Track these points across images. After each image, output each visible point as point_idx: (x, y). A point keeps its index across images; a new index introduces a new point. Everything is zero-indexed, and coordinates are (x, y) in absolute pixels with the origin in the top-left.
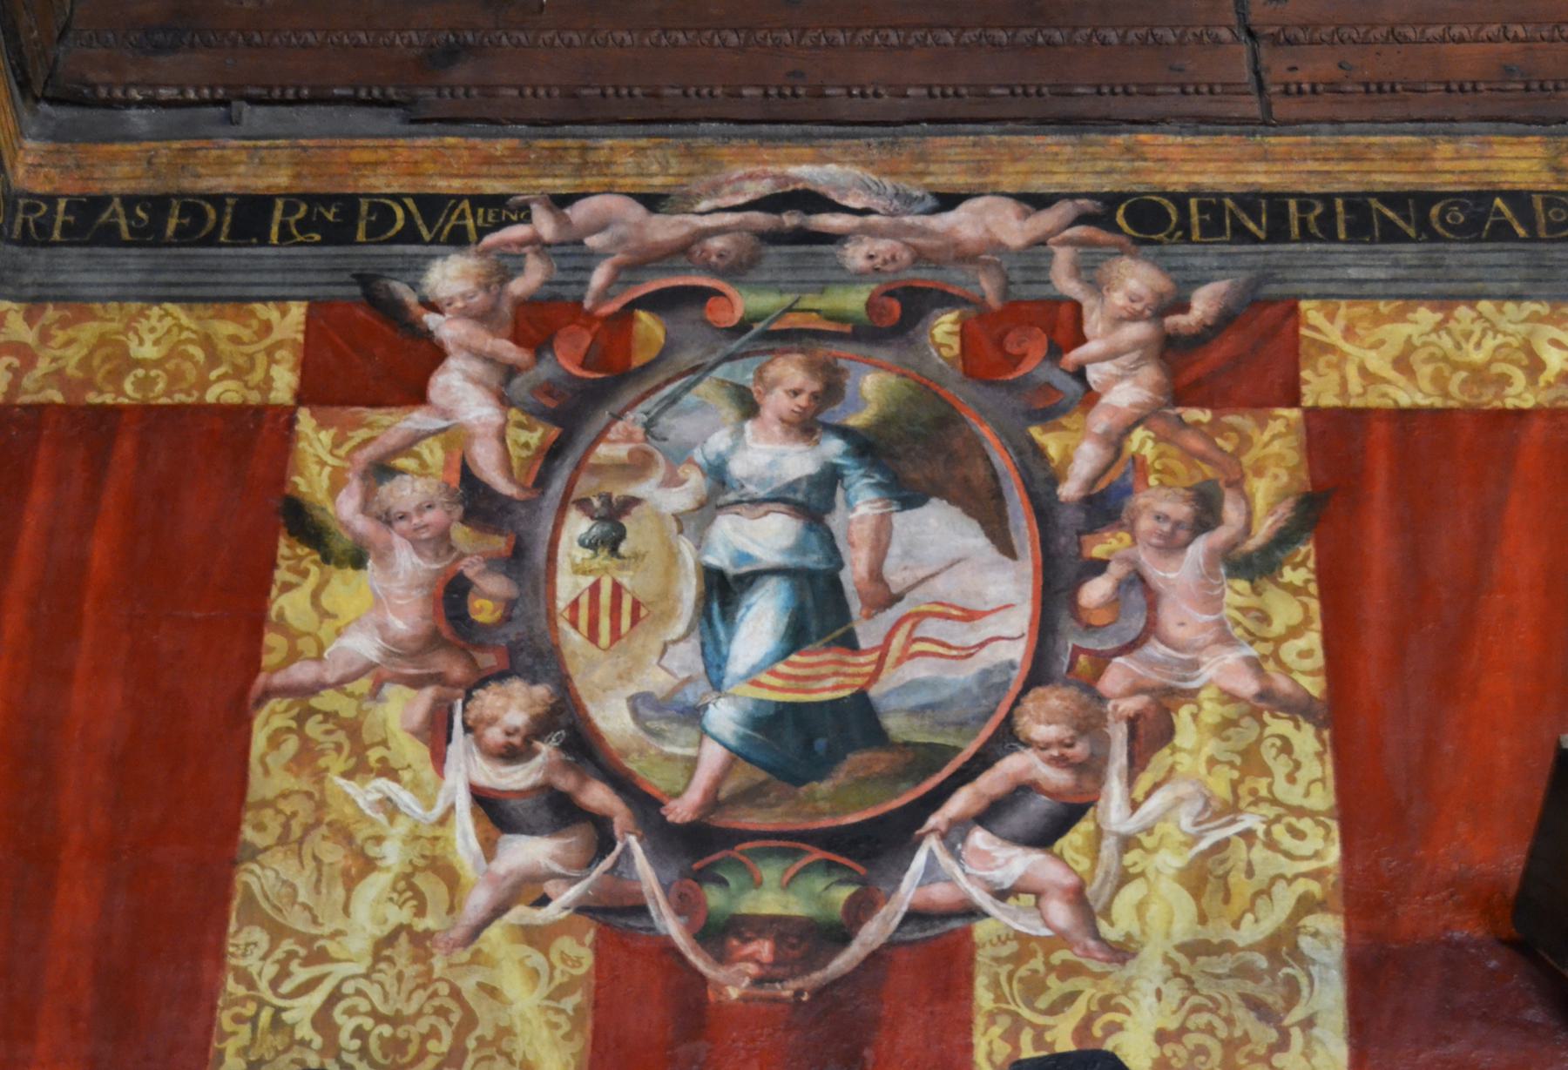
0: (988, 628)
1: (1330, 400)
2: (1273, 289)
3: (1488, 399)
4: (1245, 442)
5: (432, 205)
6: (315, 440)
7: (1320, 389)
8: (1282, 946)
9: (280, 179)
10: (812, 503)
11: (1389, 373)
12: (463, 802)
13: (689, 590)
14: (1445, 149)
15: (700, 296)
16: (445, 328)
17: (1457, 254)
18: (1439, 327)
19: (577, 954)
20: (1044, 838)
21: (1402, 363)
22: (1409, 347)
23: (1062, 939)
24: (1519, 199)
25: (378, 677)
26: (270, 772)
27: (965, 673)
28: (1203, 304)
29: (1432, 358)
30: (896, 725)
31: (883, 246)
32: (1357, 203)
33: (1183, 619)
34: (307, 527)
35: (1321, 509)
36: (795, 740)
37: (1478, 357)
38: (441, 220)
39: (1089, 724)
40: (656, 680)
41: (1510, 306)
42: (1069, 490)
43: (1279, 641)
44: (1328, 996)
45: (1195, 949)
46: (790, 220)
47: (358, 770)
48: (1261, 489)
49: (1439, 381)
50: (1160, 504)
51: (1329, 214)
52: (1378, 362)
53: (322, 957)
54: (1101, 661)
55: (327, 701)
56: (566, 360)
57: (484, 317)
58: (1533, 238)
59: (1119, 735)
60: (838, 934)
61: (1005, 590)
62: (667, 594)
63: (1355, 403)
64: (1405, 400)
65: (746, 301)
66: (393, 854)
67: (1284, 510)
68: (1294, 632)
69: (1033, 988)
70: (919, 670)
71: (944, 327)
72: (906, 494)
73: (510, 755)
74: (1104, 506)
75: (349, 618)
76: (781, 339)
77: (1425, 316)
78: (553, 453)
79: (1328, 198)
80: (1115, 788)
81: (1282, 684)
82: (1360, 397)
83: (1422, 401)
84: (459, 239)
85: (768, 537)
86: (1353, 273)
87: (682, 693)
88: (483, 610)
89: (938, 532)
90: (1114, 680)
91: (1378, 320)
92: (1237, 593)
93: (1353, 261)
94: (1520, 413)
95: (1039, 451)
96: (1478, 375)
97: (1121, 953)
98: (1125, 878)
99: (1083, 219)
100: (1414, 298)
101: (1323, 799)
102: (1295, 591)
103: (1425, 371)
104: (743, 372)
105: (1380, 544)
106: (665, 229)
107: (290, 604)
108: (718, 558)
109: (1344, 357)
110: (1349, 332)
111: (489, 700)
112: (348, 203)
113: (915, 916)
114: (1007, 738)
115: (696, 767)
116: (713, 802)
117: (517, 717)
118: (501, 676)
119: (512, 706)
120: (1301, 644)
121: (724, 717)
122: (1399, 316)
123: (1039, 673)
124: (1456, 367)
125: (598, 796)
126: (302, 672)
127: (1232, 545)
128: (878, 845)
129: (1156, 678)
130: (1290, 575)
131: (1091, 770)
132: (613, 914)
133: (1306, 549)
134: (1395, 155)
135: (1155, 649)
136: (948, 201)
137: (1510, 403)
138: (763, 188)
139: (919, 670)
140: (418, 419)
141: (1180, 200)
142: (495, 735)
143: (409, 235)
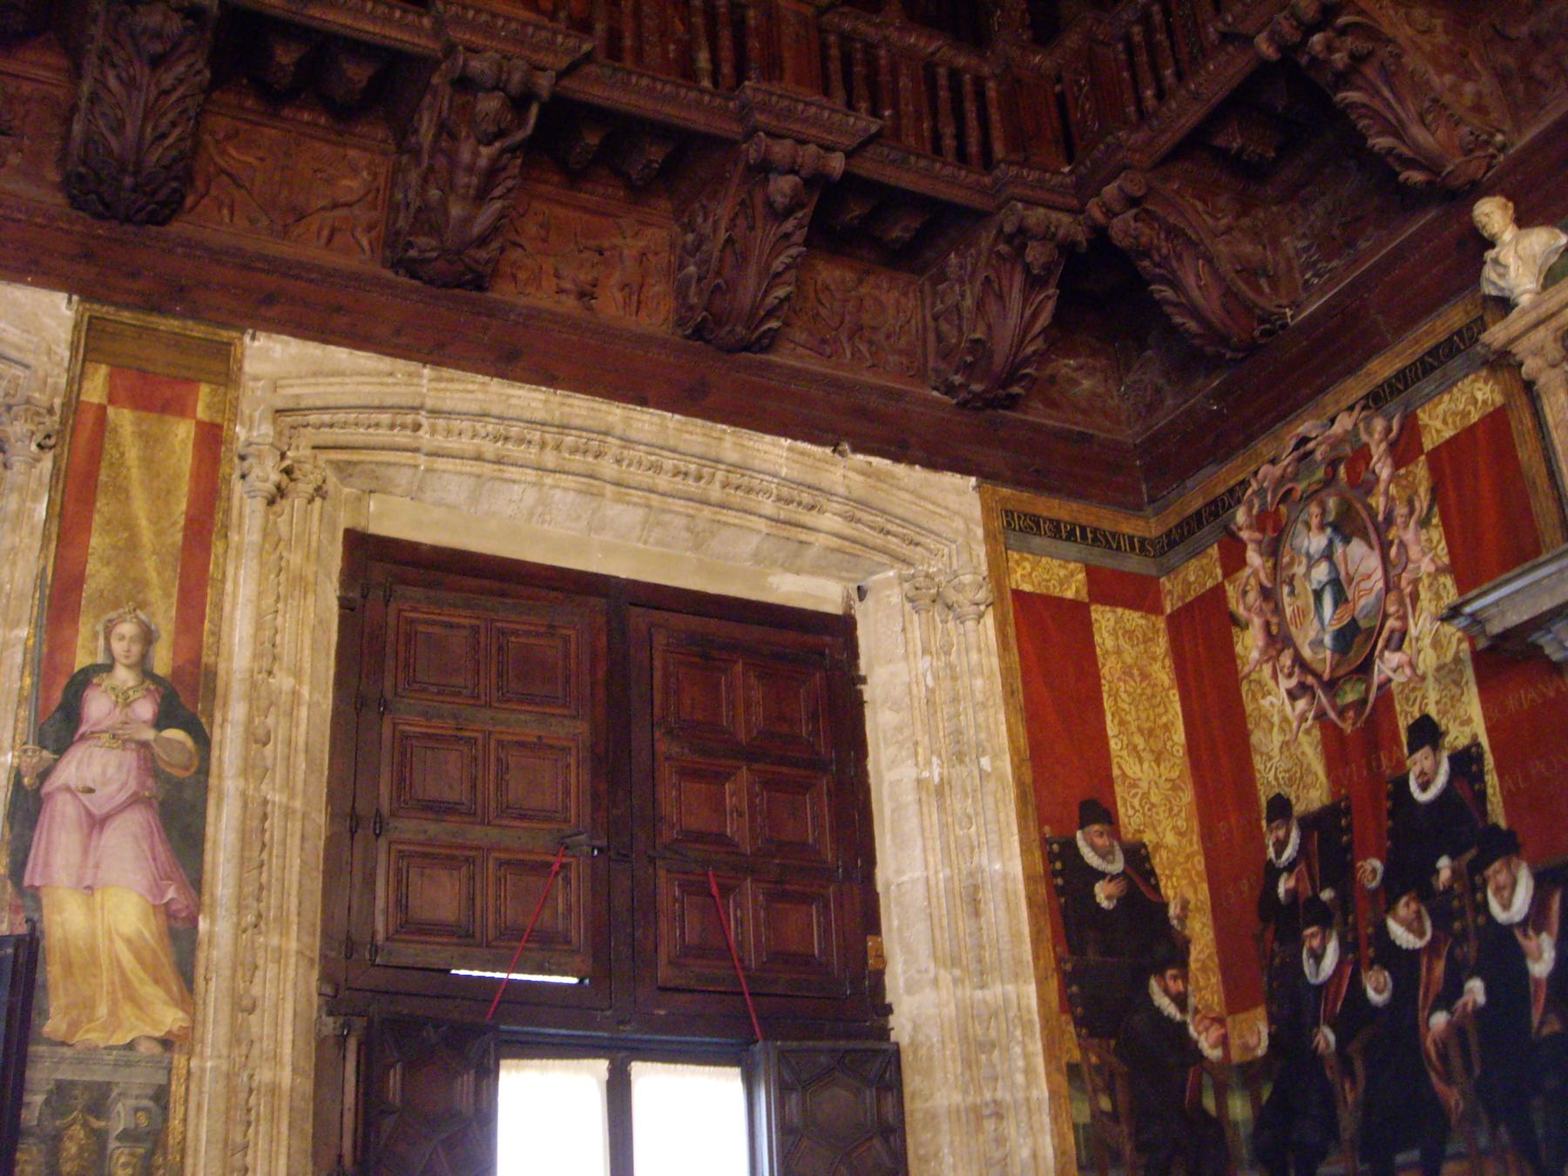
0: (1374, 578)
5: (1231, 491)
6: (1230, 590)
7: (1428, 445)
8: (1457, 660)
9: (1198, 503)
10: (1328, 555)
12: (1285, 695)
13: (1311, 600)
15: (1290, 491)
16: (1244, 535)
19: (1316, 733)
20: (1399, 648)
21: (1445, 422)
23: (1410, 680)
24: (1459, 333)
25: (1260, 663)
26: (1249, 707)
27: (1372, 598)
30: (1363, 624)
31: (1323, 448)
32: (1421, 360)
33: (1414, 552)
34: (1234, 620)
36: (1347, 636)
37: (1461, 407)
38: (1233, 496)
39: (1401, 603)
40: (1312, 634)
42: (1380, 518)
44: (1469, 673)
45: (1439, 668)
46: (1302, 450)
47: (1264, 697)
50: (1401, 510)
53: (1270, 758)
54: (1399, 576)
55: (1254, 676)
56: (1270, 534)
57: (1250, 527)
59: (1408, 600)
60: (1364, 701)
61: (1373, 562)
62: (1308, 604)
65: (1301, 487)
66: (1276, 719)
69: (1407, 699)
70: (1362, 602)
71: (1342, 470)
72: (1347, 540)
73: (1290, 675)
74: (1389, 520)
75: (1250, 644)
76: (1308, 497)
77: (1446, 397)
78: (1275, 566)
79: (1414, 363)
80: (1411, 621)
83: (1452, 433)
84: (1239, 502)
85: (1321, 572)
87: (1315, 634)
88: (1274, 630)
89: (1357, 547)
90: (1403, 583)
91: (1436, 406)
92: (1423, 535)
93: (1427, 386)
95: (1370, 506)
97: (1423, 678)
98: (1419, 652)
99: (1363, 409)
102: (1436, 526)
103: (1450, 420)
104: (1303, 516)
105: (1452, 496)
106: (1277, 471)
107: (1239, 649)
108: (1315, 586)
111: (1282, 658)
112: (1214, 502)
113: (1380, 687)
114: (1386, 616)
115: (1323, 659)
116: (1333, 670)
117: (1288, 663)
118: (1282, 650)
119: (1286, 659)
121: (1328, 640)
122: (1440, 402)
123: (1387, 589)
125: (1310, 680)
126: (1246, 669)
128: (1366, 668)
129: (1412, 576)
130: (1435, 521)
131: (1404, 618)
132: (1321, 716)
133: (1436, 509)
135: (1411, 566)
136: (1332, 421)
138: (1293, 443)
139: (1362, 602)
140: (1247, 571)
141: (1381, 386)
142: (1286, 671)
143: (1230, 507)
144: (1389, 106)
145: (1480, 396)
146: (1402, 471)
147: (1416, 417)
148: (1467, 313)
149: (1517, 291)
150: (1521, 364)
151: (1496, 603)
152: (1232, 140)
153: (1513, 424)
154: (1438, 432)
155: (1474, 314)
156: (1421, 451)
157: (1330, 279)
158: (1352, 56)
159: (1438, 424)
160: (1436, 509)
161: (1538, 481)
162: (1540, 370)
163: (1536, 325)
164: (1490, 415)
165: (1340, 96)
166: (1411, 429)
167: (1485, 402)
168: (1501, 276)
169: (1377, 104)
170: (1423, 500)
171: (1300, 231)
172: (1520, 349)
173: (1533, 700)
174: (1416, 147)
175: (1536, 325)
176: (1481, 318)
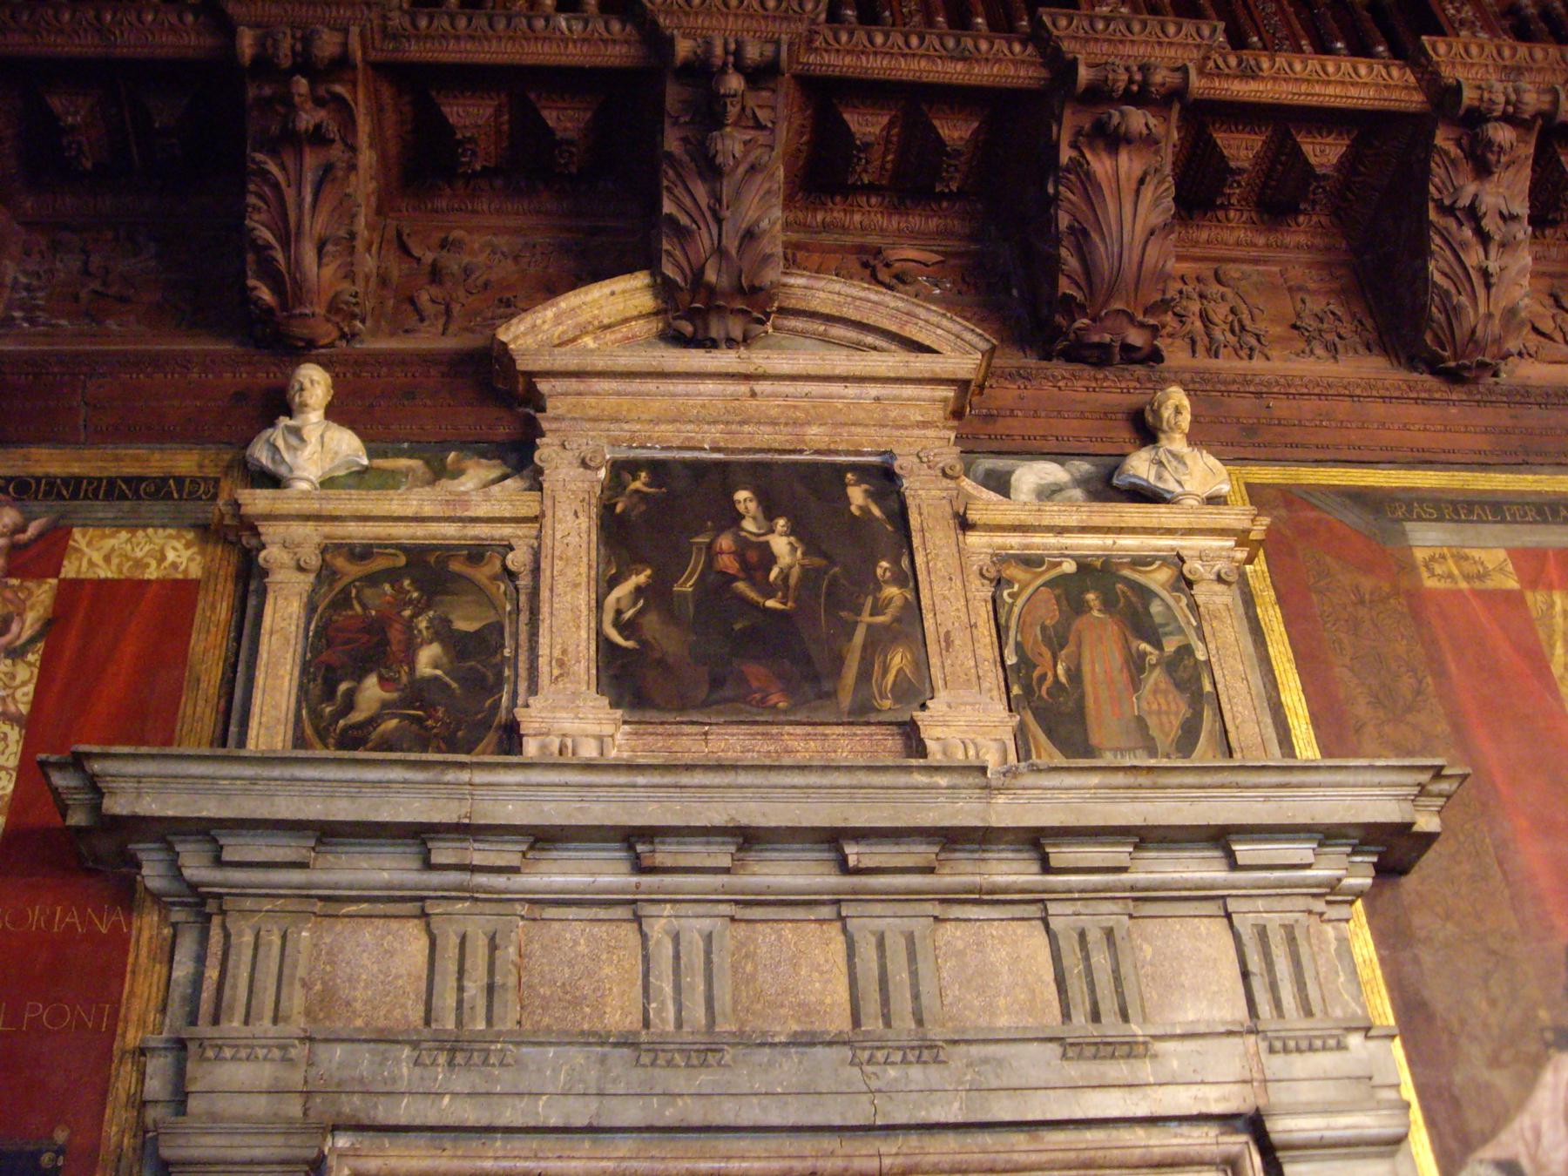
1: (72, 575)
2: (62, 522)
3: (138, 575)
4: (30, 594)
7: (69, 570)
11: (101, 562)
14: (157, 456)
17: (147, 507)
18: (129, 541)
21: (107, 559)
22: (113, 549)
24: (180, 480)
28: (32, 530)
29: (121, 555)
32: (112, 482)
35: (51, 628)
37: (139, 554)
41: (160, 531)
43: (16, 688)
48: (31, 617)
49: (120, 566)
51: (99, 487)
52: (97, 557)
58: (181, 498)
63: (82, 576)
64: (103, 575)
67: (37, 627)
68: (24, 684)
77: (124, 535)
79: (100, 479)
81: (12, 708)
82: (87, 573)
83: (110, 575)
86: (100, 515)
91: (103, 537)
93: (102, 510)
94: (149, 581)
96: (140, 564)
100: (122, 527)
101: (13, 762)
102: (30, 664)
103: (115, 561)
105: (72, 642)
109: (84, 554)
110: (89, 544)
120: (25, 689)
122: (112, 536)
124: (128, 558)
127: (11, 643)
130: (31, 657)
133: (41, 645)
134: (137, 458)
137: (146, 576)
141: (38, 480)
144: (300, 206)
145: (171, 556)
146: (15, 582)
147: (69, 533)
148: (201, 466)
149: (297, 473)
150: (263, 546)
151: (139, 778)
152: (72, 110)
153: (200, 605)
154: (91, 563)
155: (211, 472)
156: (56, 574)
157: (45, 334)
158: (318, 127)
159: (97, 557)
160: (41, 645)
161: (204, 678)
162: (282, 566)
163: (307, 518)
164: (176, 581)
165: (259, 157)
166: (54, 545)
167: (174, 565)
168: (289, 447)
169: (290, 195)
170: (31, 621)
171: (31, 267)
172: (269, 531)
173: (72, 927)
174: (296, 264)
175: (307, 518)
176: (217, 481)
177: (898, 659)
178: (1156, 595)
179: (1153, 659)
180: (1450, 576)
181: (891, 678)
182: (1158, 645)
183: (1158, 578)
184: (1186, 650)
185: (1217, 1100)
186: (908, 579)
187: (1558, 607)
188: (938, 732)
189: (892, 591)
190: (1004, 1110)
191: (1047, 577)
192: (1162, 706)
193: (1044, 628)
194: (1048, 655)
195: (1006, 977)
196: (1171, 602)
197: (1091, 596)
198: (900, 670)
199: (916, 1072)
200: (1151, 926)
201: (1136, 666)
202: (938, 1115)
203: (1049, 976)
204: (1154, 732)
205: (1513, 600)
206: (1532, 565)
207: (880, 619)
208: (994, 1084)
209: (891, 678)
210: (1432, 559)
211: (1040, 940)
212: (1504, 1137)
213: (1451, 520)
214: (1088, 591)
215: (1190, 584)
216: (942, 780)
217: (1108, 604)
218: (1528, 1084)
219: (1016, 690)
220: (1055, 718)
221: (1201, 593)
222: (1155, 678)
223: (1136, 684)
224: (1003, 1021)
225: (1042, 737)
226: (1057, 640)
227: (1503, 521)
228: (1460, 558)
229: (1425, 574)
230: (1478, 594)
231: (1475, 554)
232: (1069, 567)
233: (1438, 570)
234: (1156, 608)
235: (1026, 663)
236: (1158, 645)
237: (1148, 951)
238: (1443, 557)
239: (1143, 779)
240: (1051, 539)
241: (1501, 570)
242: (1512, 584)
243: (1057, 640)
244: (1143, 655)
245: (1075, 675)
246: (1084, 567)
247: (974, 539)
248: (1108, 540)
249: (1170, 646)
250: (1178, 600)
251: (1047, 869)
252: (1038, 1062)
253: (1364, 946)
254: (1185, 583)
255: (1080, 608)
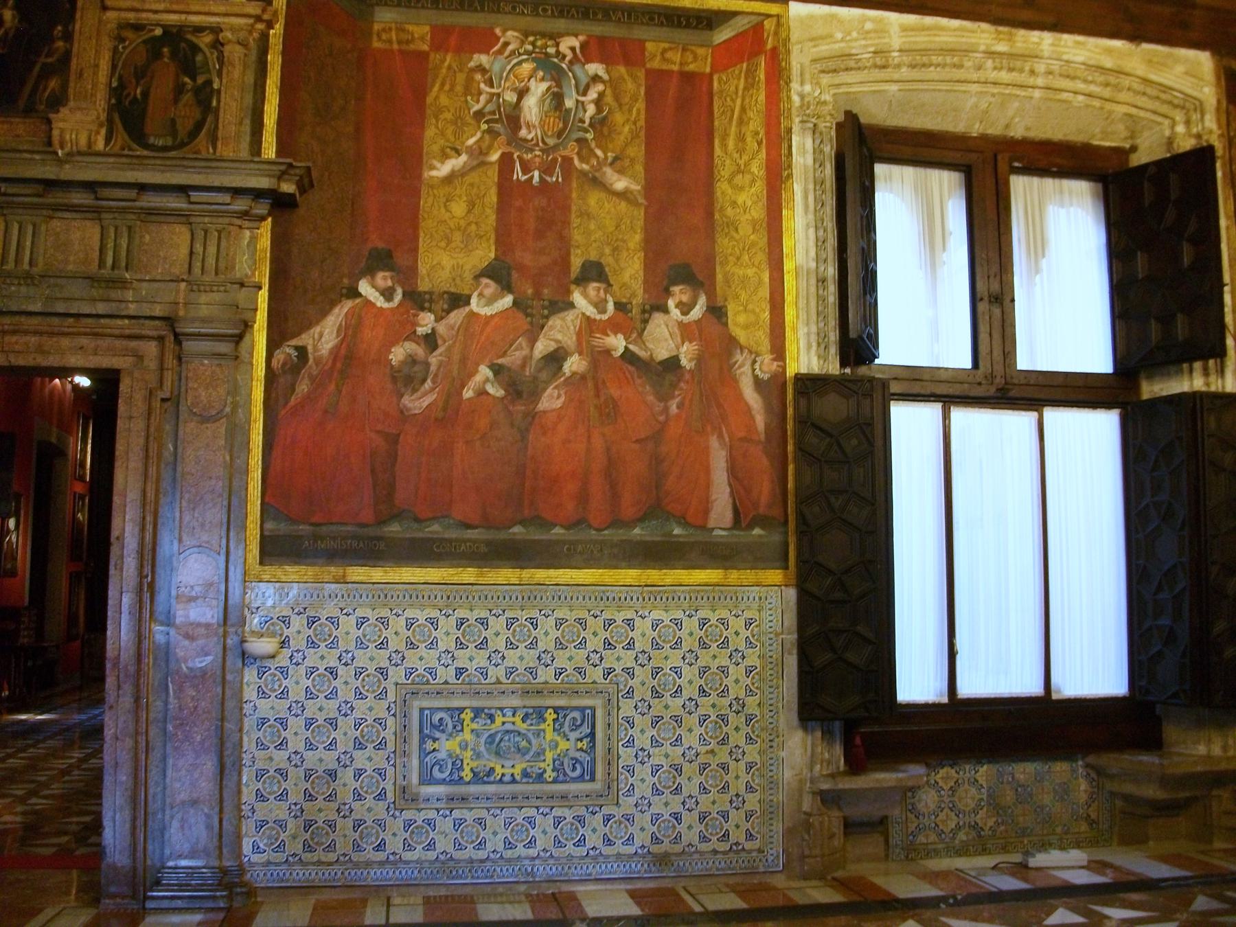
177: (53, 84)
178: (200, 50)
179: (189, 87)
180: (390, 41)
181: (46, 94)
182: (194, 79)
183: (205, 40)
184: (209, 83)
185: (158, 311)
186: (68, 37)
187: (446, 64)
188: (61, 125)
189: (60, 44)
190: (60, 308)
191: (145, 37)
192: (186, 112)
193: (136, 68)
194: (134, 81)
195: (76, 247)
196: (208, 54)
197: (165, 50)
198: (53, 90)
199: (23, 289)
200: (153, 227)
201: (179, 90)
202: (31, 308)
203: (97, 248)
204: (179, 127)
205: (422, 57)
206: (441, 37)
207: (50, 60)
208: (59, 295)
209: (46, 94)
210: (384, 30)
211: (97, 230)
212: (303, 336)
213: (406, 6)
214: (164, 46)
215: (222, 45)
216: (37, 157)
217: (174, 55)
218: (324, 313)
219: (113, 101)
220: (128, 116)
221: (227, 49)
222: (188, 97)
223: (176, 101)
224: (70, 267)
225: (120, 126)
226: (141, 74)
227: (437, 8)
228: (401, 30)
229: (375, 38)
230: (401, 52)
231: (410, 28)
232: (158, 32)
233: (384, 37)
234: (199, 58)
235: (122, 86)
236: (194, 79)
237: (147, 237)
238: (390, 29)
239: (135, 161)
240: (152, 16)
241: (422, 39)
242: (426, 48)
243: (141, 74)
244: (184, 84)
245: (145, 94)
246: (167, 29)
247: (111, 15)
248: (183, 17)
249: (200, 80)
250: (212, 54)
251: (97, 199)
252: (76, 289)
253: (265, 242)
254: (217, 45)
255: (156, 55)
